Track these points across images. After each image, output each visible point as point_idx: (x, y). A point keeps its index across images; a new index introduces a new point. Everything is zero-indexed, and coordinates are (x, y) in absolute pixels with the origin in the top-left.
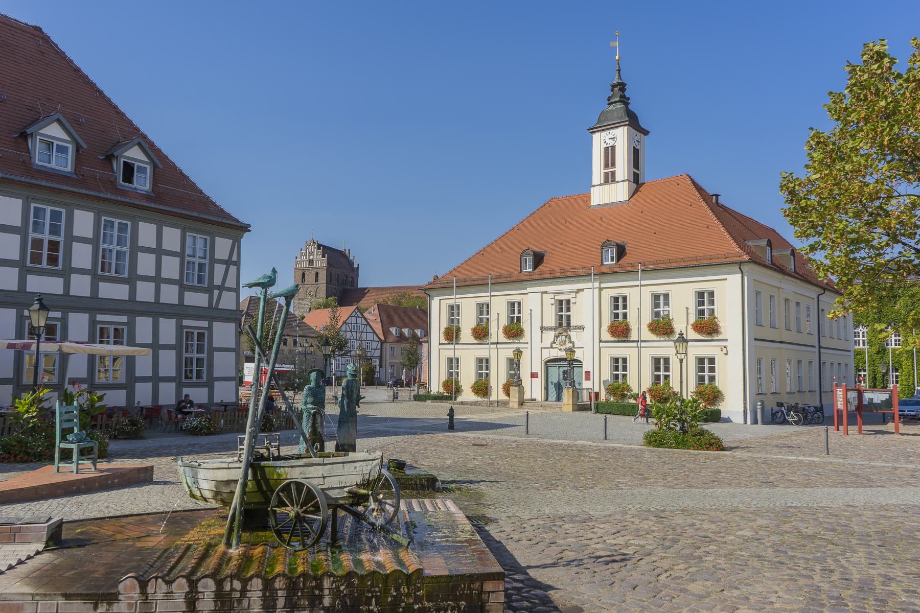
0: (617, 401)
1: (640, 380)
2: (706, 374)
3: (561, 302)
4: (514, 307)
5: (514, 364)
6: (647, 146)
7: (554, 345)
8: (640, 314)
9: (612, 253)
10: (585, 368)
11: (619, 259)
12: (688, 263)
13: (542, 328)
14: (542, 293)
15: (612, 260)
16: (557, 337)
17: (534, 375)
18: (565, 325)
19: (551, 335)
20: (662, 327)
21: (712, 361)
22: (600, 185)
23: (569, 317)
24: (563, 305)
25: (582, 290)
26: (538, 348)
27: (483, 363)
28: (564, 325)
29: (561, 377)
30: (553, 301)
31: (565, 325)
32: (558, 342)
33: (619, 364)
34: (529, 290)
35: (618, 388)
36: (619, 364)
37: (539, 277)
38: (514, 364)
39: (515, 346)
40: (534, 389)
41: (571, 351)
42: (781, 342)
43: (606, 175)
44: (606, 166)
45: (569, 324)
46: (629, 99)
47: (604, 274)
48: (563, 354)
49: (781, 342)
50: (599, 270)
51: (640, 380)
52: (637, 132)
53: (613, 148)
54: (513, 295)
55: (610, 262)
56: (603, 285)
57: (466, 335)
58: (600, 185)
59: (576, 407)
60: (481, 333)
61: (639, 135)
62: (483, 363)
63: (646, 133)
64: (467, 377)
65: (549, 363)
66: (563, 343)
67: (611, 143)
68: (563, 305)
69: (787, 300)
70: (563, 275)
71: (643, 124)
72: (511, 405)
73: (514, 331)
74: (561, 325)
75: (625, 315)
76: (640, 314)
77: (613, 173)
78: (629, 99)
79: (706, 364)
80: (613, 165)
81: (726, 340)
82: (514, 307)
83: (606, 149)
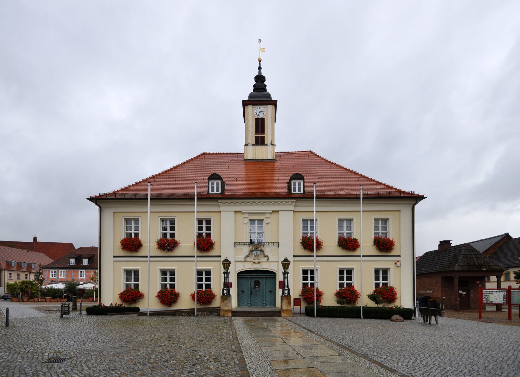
4: (204, 224)
7: (248, 259)
14: (235, 212)
16: (251, 251)
19: (246, 250)
20: (348, 244)
25: (278, 211)
27: (168, 275)
29: (253, 286)
30: (247, 220)
56: (298, 209)
60: (168, 244)
62: (168, 275)
64: (150, 286)
65: (241, 275)
73: (205, 245)
82: (204, 224)
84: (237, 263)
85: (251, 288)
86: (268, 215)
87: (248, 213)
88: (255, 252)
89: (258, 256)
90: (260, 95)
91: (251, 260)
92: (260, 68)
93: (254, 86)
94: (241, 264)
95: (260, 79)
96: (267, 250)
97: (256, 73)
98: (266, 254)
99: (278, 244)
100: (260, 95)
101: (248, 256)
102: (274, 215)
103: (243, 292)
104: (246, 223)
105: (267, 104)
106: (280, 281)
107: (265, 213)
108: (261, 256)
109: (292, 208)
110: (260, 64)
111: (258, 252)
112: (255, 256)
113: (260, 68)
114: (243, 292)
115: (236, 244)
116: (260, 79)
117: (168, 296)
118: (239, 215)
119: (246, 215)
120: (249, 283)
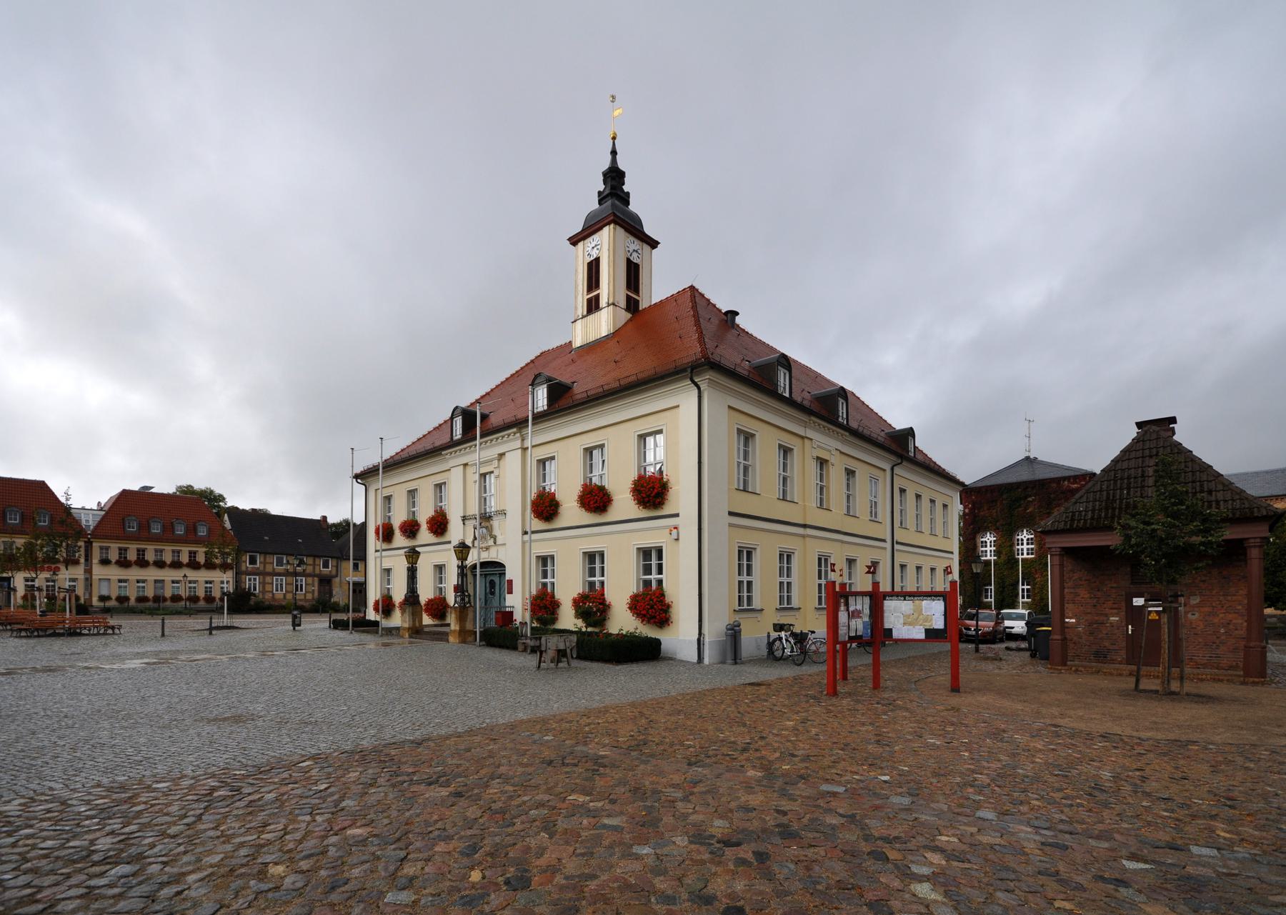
21: (660, 552)
42: (805, 526)
43: (589, 301)
44: (590, 289)
49: (805, 526)
52: (632, 238)
53: (597, 260)
58: (583, 317)
61: (634, 244)
63: (653, 244)
67: (595, 254)
69: (822, 462)
71: (648, 230)
77: (597, 297)
79: (650, 557)
80: (597, 286)
81: (677, 515)
92: (614, 153)
93: (600, 193)
95: (614, 176)
113: (614, 153)
116: (614, 176)
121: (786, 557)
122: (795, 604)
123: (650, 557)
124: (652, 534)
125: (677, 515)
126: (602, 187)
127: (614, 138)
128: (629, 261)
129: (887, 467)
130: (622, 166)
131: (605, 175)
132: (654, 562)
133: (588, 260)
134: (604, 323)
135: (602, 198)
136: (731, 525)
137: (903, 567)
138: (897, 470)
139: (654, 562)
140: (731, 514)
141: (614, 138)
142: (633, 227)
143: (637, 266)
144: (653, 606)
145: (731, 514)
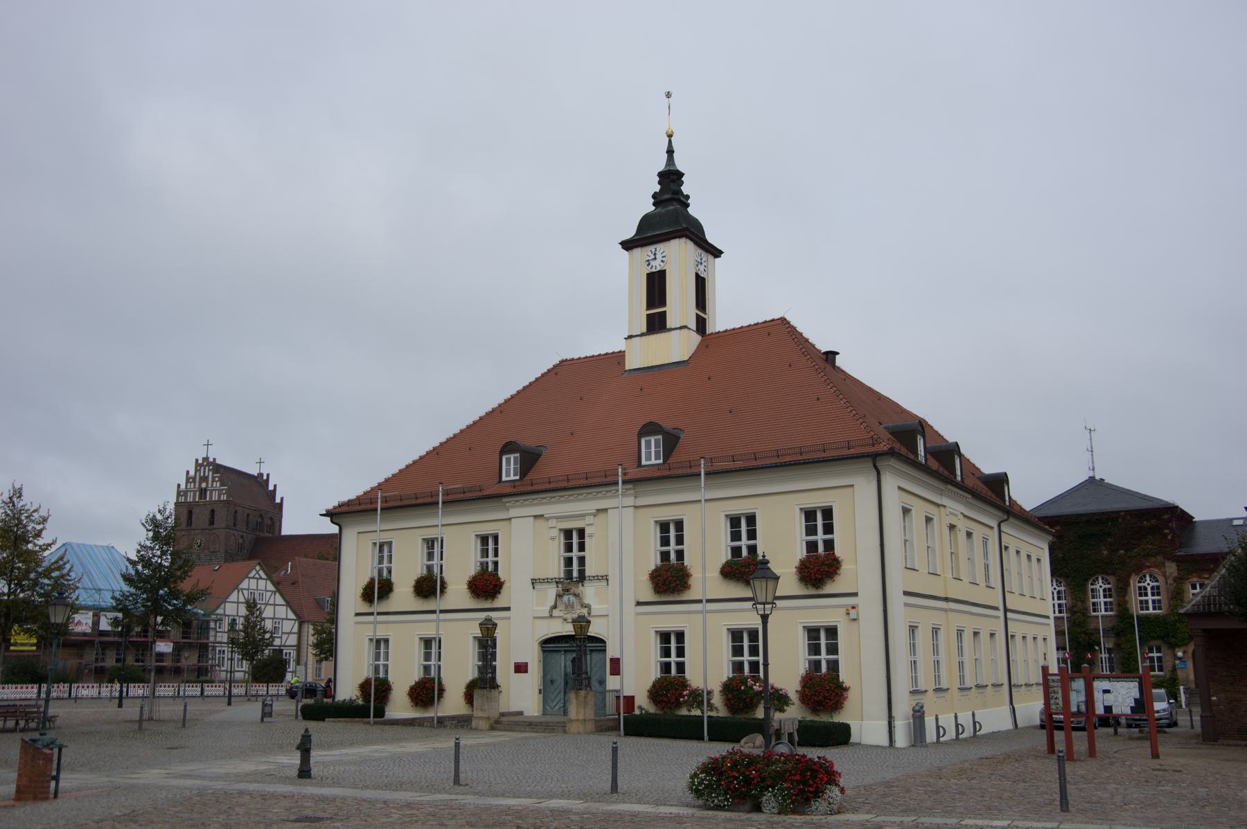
0: (669, 711)
1: (709, 668)
2: (824, 656)
3: (568, 534)
5: (487, 644)
6: (721, 274)
7: (556, 613)
8: (707, 551)
9: (657, 446)
10: (612, 652)
11: (666, 458)
12: (787, 459)
13: (534, 582)
14: (535, 517)
15: (657, 458)
16: (559, 596)
17: (521, 668)
18: (575, 574)
19: (552, 592)
21: (832, 632)
22: (642, 335)
23: (582, 560)
24: (574, 538)
25: (606, 510)
26: (527, 621)
28: (573, 577)
30: (555, 533)
31: (575, 574)
32: (561, 607)
33: (671, 641)
34: (513, 512)
35: (670, 688)
36: (671, 641)
37: (530, 488)
38: (487, 644)
39: (483, 615)
40: (522, 694)
41: (582, 622)
42: (946, 599)
43: (650, 318)
44: (650, 305)
45: (582, 577)
46: (688, 197)
47: (641, 480)
48: (568, 629)
50: (634, 473)
51: (709, 668)
53: (662, 274)
54: (484, 519)
55: (653, 461)
57: (403, 595)
59: (590, 726)
63: (716, 253)
64: (404, 673)
65: (550, 645)
66: (569, 606)
67: (657, 266)
68: (574, 538)
70: (572, 484)
71: (711, 238)
72: (474, 724)
73: (486, 585)
74: (569, 574)
75: (680, 555)
76: (707, 551)
78: (688, 197)
79: (822, 638)
80: (663, 302)
81: (855, 594)
83: (650, 276)
84: (539, 622)
85: (566, 675)
86: (590, 519)
87: (556, 518)
88: (565, 598)
89: (572, 606)
90: (671, 215)
91: (561, 614)
92: (670, 152)
93: (655, 196)
94: (545, 622)
95: (671, 178)
96: (589, 592)
97: (661, 166)
98: (586, 601)
99: (605, 578)
100: (671, 215)
101: (555, 607)
102: (601, 516)
103: (552, 682)
104: (553, 539)
105: (669, 239)
106: (611, 660)
107: (584, 516)
108: (577, 606)
109: (630, 501)
110: (670, 142)
111: (572, 598)
112: (566, 607)
113: (670, 152)
114: (552, 682)
115: (534, 582)
116: (671, 178)
117: (426, 692)
118: (540, 522)
119: (552, 523)
120: (563, 662)
121: (935, 631)
122: (944, 686)
123: (822, 638)
124: (822, 613)
125: (855, 594)
126: (657, 188)
127: (670, 136)
128: (697, 275)
129: (994, 524)
130: (680, 165)
131: (661, 175)
132: (673, 645)
133: (649, 270)
134: (676, 346)
135: (658, 199)
136: (906, 605)
137: (1013, 636)
138: (1004, 528)
139: (673, 645)
140: (906, 593)
141: (670, 136)
142: (694, 233)
143: (703, 279)
144: (824, 690)
145: (906, 593)
